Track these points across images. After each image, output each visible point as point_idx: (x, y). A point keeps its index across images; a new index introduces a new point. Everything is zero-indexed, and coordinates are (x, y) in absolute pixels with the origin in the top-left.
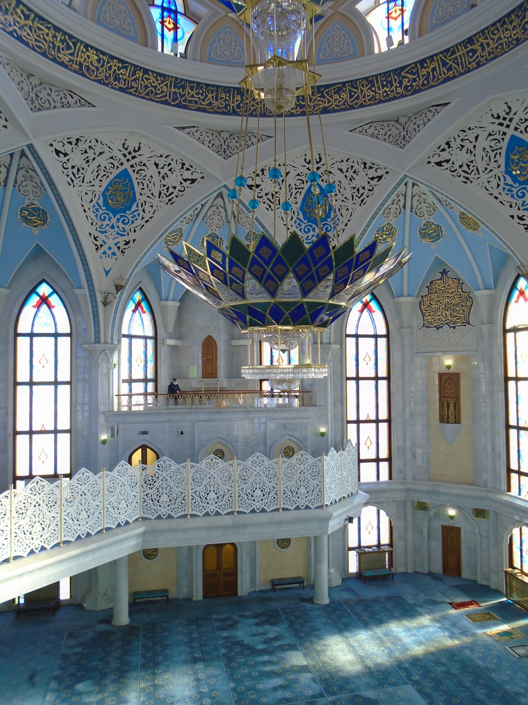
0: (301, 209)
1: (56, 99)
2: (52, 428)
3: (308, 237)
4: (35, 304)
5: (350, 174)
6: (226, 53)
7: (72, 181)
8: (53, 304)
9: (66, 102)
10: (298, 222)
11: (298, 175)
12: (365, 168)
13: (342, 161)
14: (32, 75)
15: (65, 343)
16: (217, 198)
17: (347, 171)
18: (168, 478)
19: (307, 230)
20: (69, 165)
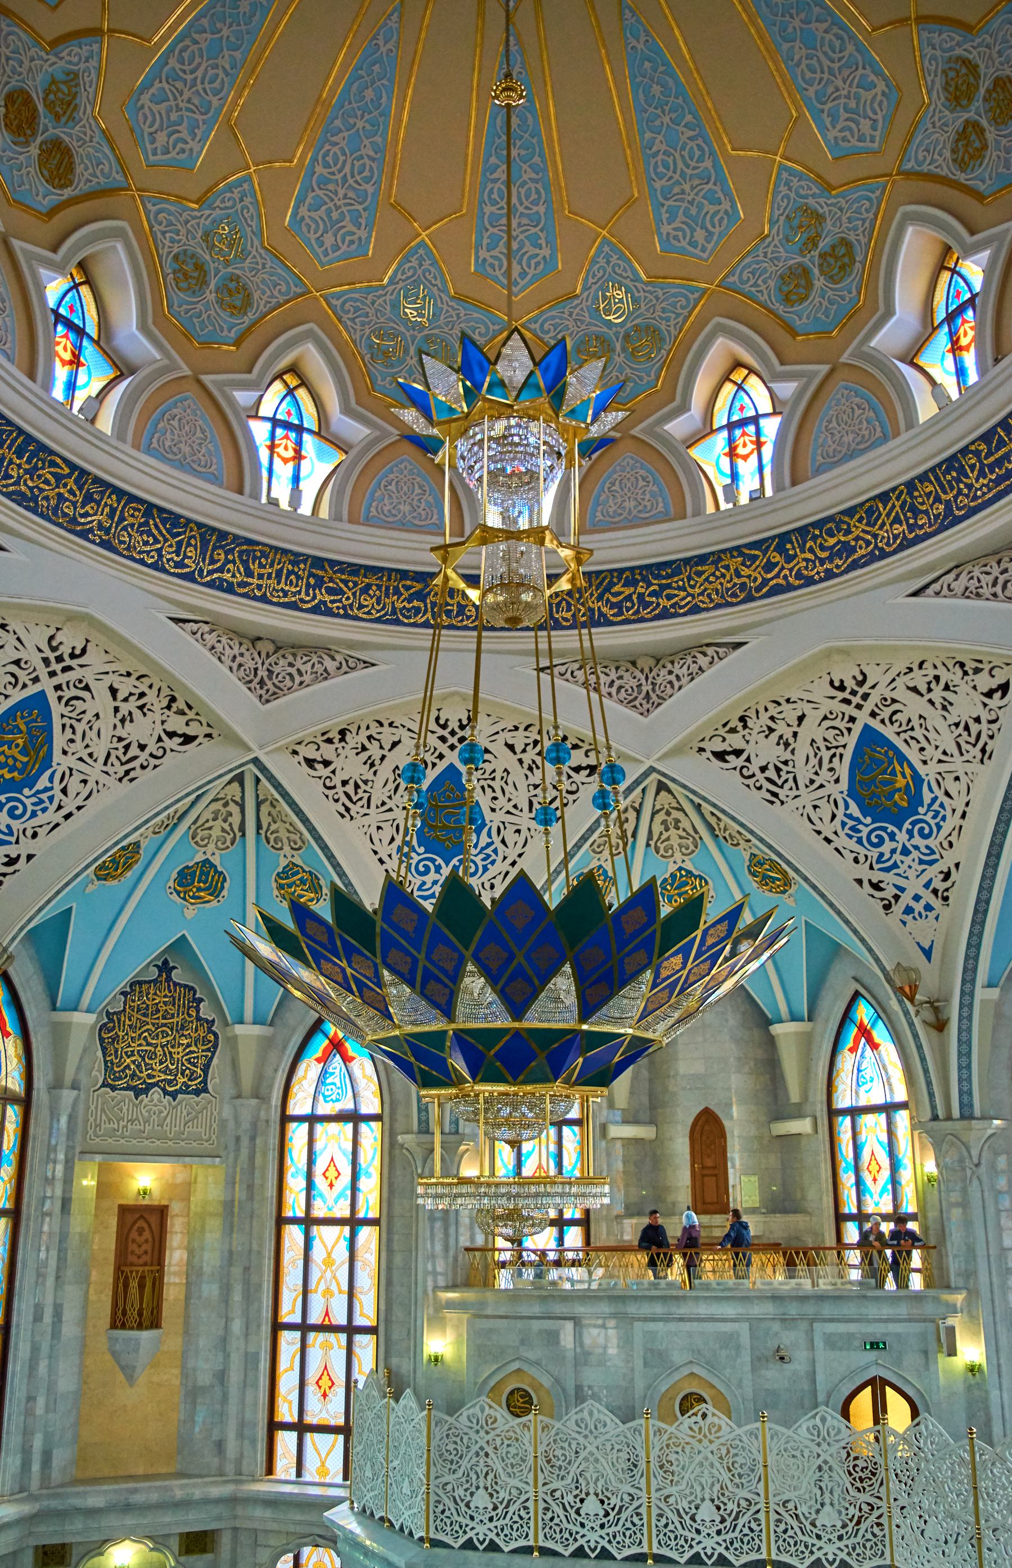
0: (852, 793)
1: (303, 669)
2: (343, 1321)
3: (882, 855)
4: (319, 1054)
5: (938, 694)
6: (626, 504)
7: (348, 810)
8: (351, 1053)
9: (321, 670)
10: (851, 823)
11: (825, 718)
12: (966, 673)
13: (911, 670)
14: (259, 639)
15: (371, 1134)
16: (657, 793)
17: (930, 690)
18: (489, 1450)
19: (875, 840)
20: (337, 781)
